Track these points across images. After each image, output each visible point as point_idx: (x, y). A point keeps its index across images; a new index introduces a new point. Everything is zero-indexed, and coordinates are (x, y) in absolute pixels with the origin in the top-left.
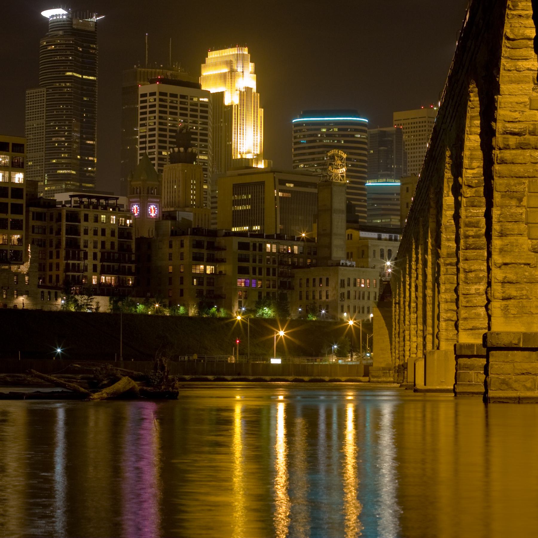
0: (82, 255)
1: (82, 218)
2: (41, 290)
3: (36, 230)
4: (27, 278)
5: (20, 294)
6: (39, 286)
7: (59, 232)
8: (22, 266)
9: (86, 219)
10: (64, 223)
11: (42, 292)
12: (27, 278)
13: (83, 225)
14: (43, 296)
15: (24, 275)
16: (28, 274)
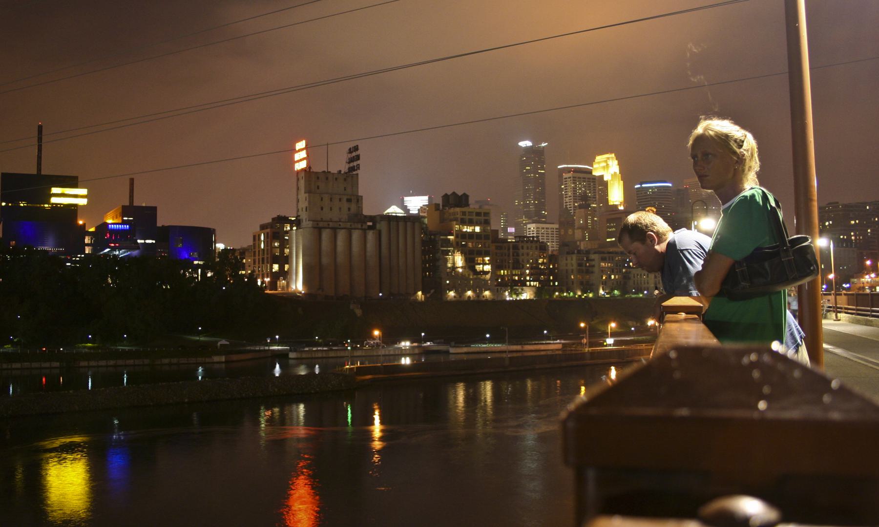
0: (521, 266)
1: (520, 248)
2: (497, 287)
3: (498, 255)
4: (489, 282)
5: (486, 290)
6: (496, 286)
7: (509, 256)
8: (487, 276)
9: (523, 248)
10: (511, 250)
11: (498, 289)
12: (489, 282)
13: (521, 251)
14: (498, 291)
15: (488, 280)
16: (489, 280)
